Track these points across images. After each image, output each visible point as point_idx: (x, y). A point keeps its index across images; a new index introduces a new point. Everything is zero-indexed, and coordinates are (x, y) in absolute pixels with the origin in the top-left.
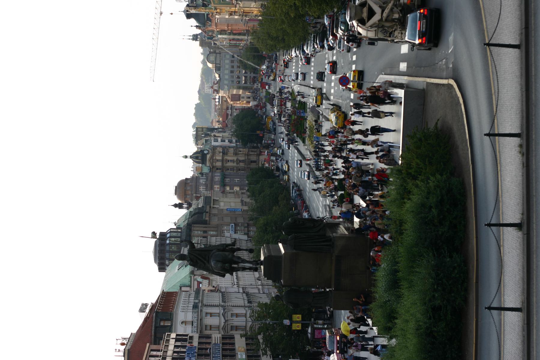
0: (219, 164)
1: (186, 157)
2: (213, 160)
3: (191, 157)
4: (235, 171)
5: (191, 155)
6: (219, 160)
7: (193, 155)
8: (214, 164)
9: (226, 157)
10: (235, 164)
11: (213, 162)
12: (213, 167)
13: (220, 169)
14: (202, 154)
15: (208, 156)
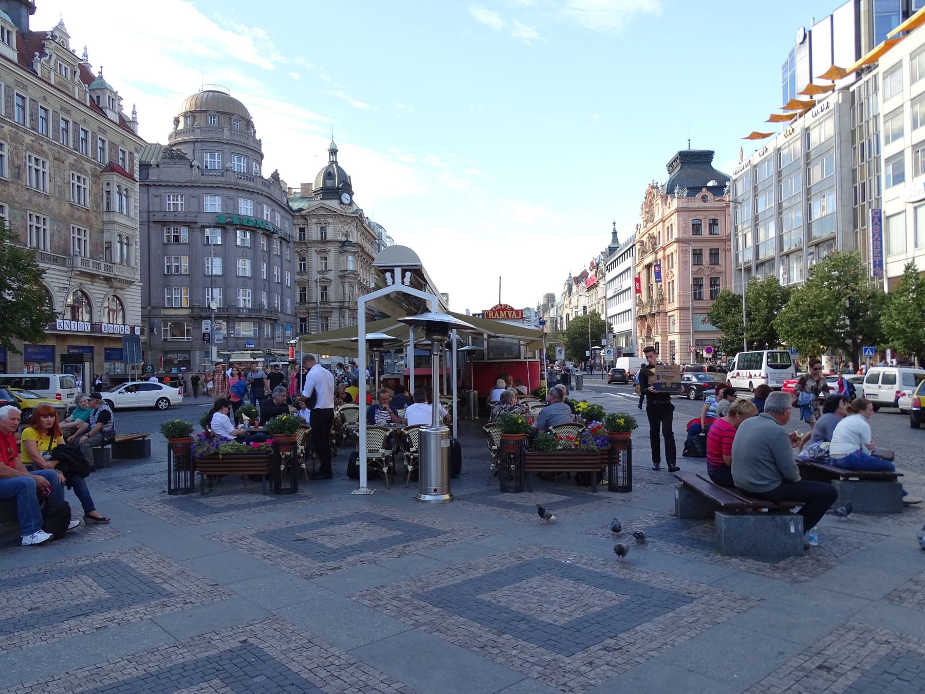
0: (314, 233)
1: (333, 152)
2: (325, 216)
3: (334, 162)
4: (298, 277)
5: (339, 164)
6: (325, 236)
7: (338, 167)
8: (314, 221)
9: (333, 251)
10: (315, 276)
11: (318, 216)
12: (304, 217)
13: (302, 237)
14: (338, 188)
15: (333, 204)
